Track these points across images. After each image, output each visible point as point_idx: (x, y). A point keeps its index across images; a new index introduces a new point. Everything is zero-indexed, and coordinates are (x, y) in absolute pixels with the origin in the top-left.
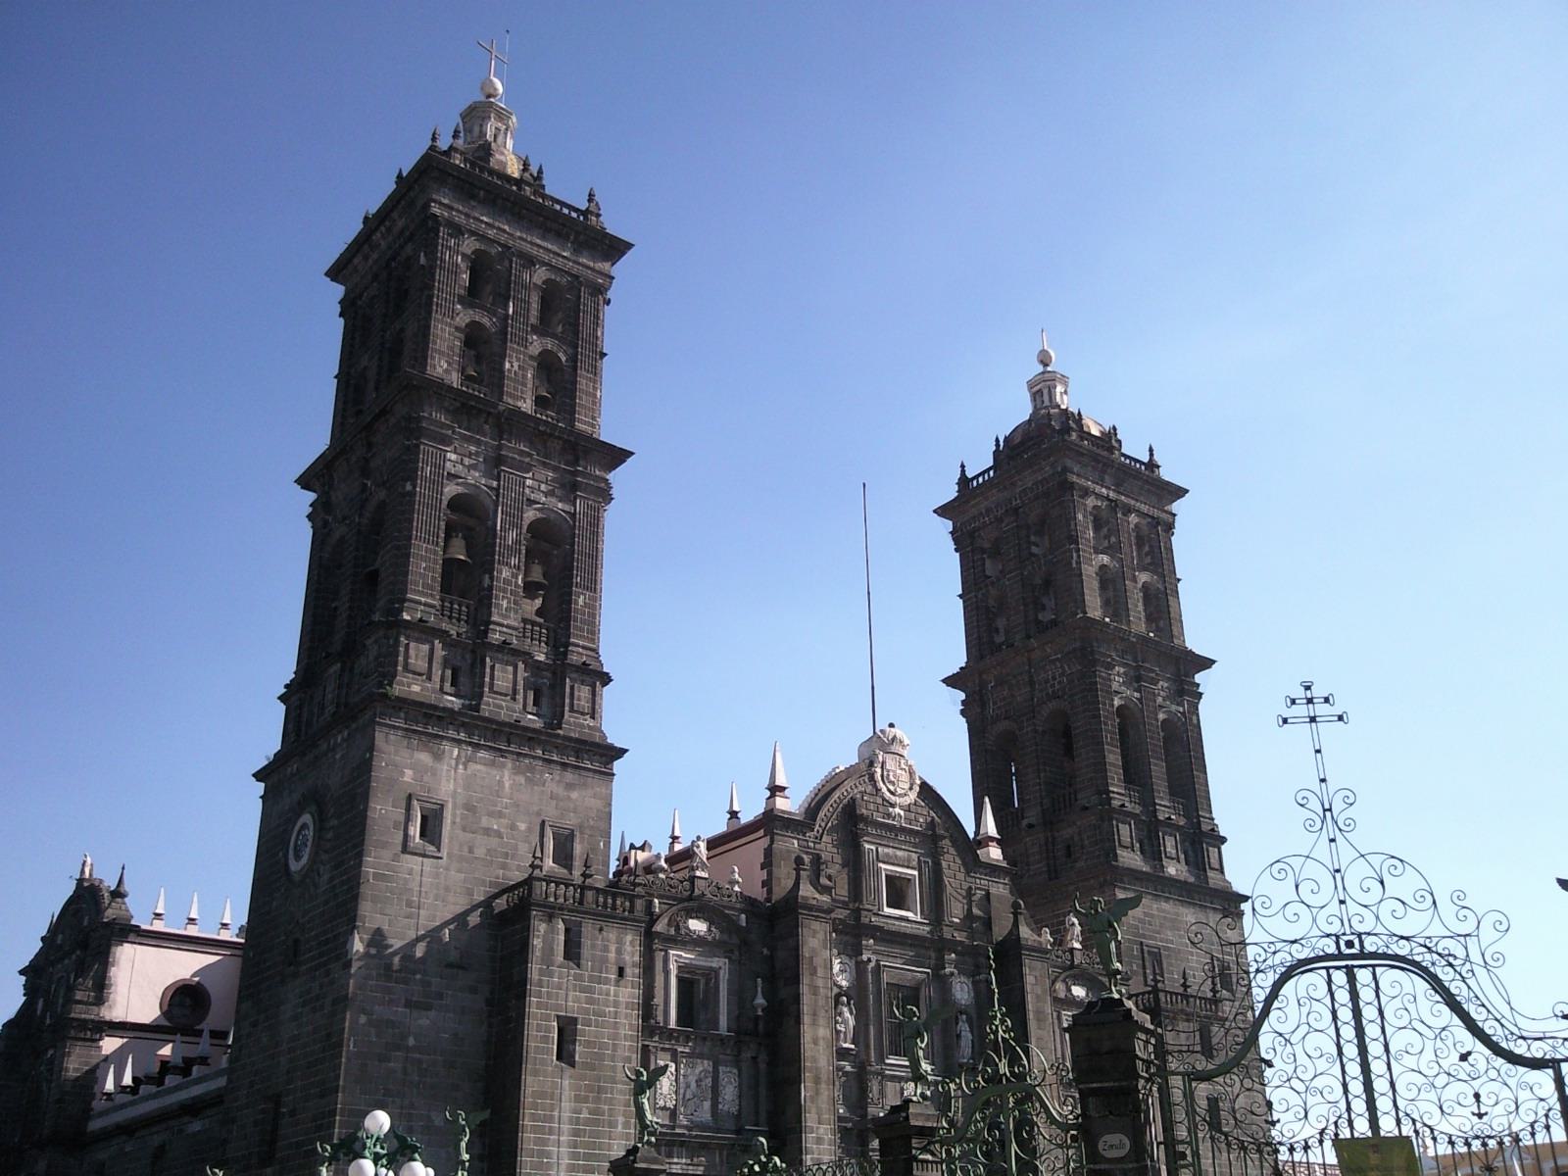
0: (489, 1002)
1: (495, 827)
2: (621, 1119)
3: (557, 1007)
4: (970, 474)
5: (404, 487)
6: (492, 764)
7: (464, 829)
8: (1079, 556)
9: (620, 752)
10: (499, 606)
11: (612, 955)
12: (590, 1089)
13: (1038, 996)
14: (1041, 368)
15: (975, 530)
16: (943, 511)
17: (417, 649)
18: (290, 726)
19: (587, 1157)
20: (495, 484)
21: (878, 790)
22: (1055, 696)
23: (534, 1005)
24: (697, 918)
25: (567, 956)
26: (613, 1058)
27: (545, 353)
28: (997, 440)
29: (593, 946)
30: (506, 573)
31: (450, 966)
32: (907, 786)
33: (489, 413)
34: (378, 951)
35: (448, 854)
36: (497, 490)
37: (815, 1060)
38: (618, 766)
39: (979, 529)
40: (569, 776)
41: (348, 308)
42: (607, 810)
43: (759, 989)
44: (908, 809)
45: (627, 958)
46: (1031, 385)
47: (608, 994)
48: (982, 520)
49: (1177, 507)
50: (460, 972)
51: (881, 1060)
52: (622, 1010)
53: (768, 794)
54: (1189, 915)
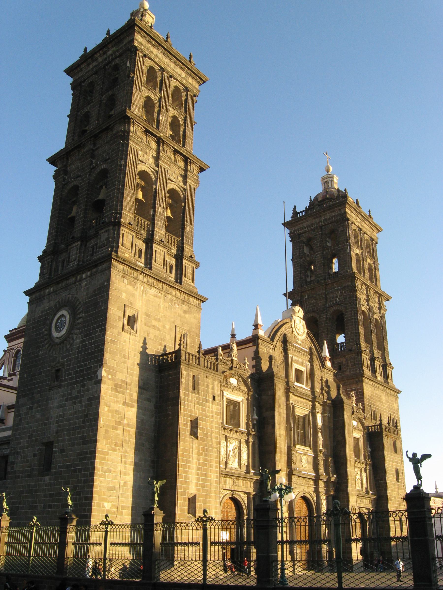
0: (156, 406)
1: (157, 326)
2: (214, 464)
3: (191, 411)
4: (298, 211)
5: (120, 162)
6: (156, 296)
7: (145, 325)
8: (350, 248)
10: (158, 224)
11: (210, 390)
12: (203, 449)
13: (348, 424)
14: (326, 173)
15: (301, 234)
16: (287, 225)
17: (127, 237)
18: (45, 271)
19: (203, 480)
21: (293, 332)
22: (337, 304)
23: (182, 409)
25: (194, 388)
26: (211, 436)
27: (174, 117)
28: (310, 198)
29: (204, 385)
32: (303, 332)
33: (156, 136)
34: (112, 377)
35: (139, 335)
36: (157, 172)
37: (280, 444)
39: (303, 233)
40: (185, 307)
41: (74, 86)
42: (198, 325)
43: (255, 412)
46: (323, 179)
47: (209, 408)
48: (304, 230)
50: (145, 391)
51: (295, 446)
52: (214, 415)
53: (254, 328)
54: (384, 397)
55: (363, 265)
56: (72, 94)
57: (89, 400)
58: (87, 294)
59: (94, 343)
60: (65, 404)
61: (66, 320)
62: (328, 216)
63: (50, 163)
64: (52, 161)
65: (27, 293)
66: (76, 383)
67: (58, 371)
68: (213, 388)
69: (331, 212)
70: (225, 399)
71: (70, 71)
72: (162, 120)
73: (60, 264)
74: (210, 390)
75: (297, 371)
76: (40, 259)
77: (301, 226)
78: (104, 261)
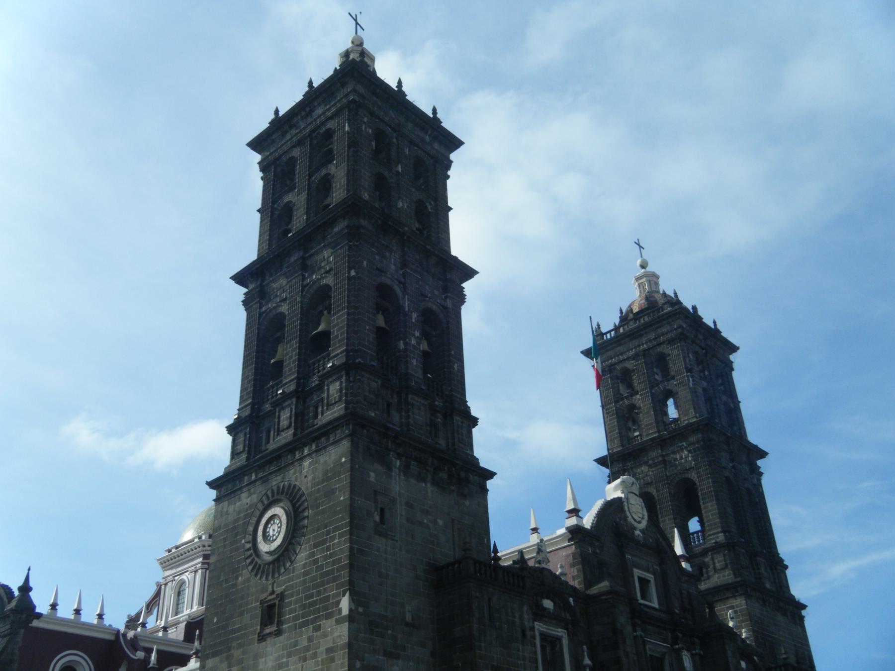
5: (349, 273)
7: (408, 521)
9: (491, 475)
11: (517, 620)
15: (611, 365)
20: (403, 280)
24: (547, 598)
30: (413, 342)
31: (407, 624)
36: (404, 284)
38: (490, 484)
39: (615, 364)
41: (264, 167)
44: (642, 531)
45: (526, 623)
47: (519, 650)
49: (732, 357)
54: (781, 618)
55: (717, 405)
56: (262, 178)
57: (329, 650)
58: (314, 479)
59: (331, 556)
60: (288, 662)
61: (281, 522)
62: (652, 336)
63: (237, 283)
64: (240, 278)
65: (212, 484)
66: (305, 624)
67: (271, 607)
68: (521, 617)
69: (657, 328)
70: (537, 634)
71: (256, 144)
72: (402, 208)
73: (264, 435)
74: (517, 620)
75: (641, 580)
76: (231, 429)
77: (611, 353)
78: (338, 426)
